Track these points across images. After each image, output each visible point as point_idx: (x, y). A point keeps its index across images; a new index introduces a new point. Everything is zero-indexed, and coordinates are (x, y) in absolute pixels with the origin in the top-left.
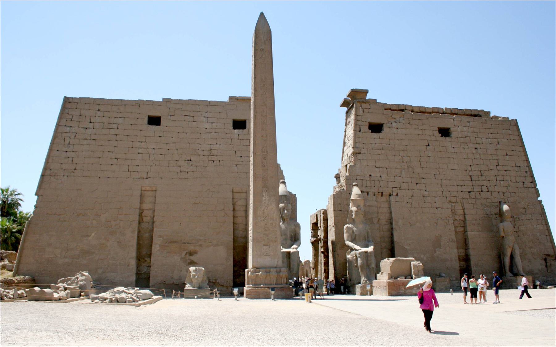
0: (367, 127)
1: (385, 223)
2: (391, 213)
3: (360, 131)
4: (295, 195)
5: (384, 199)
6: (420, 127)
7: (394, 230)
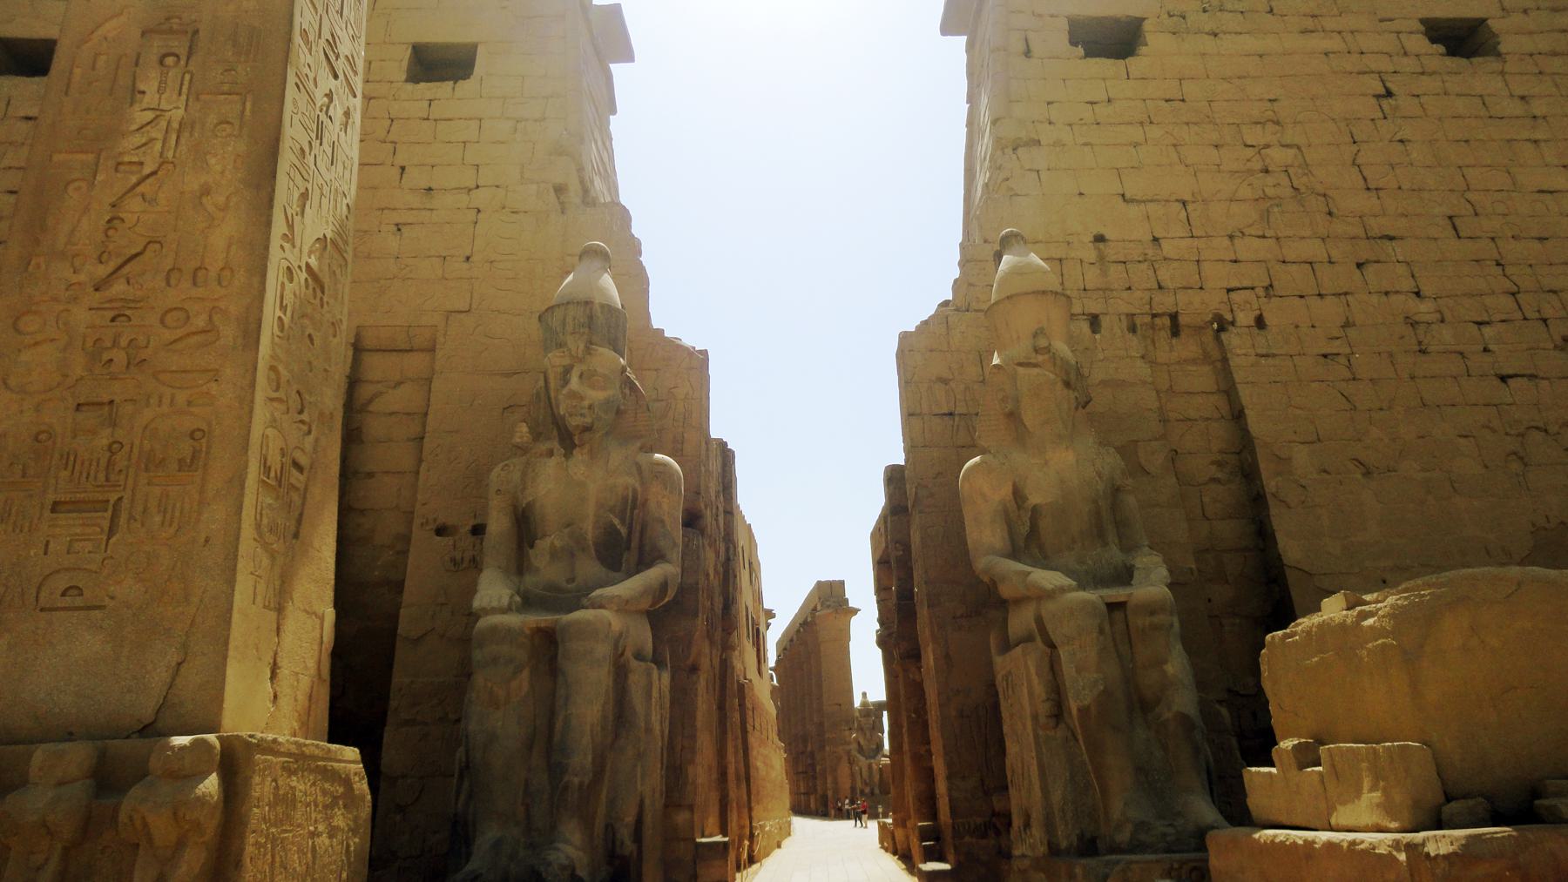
0: (1065, 37)
1: (1214, 471)
2: (1238, 416)
3: (1028, 53)
4: (704, 353)
5: (1188, 347)
6: (1330, 24)
7: (1271, 502)
